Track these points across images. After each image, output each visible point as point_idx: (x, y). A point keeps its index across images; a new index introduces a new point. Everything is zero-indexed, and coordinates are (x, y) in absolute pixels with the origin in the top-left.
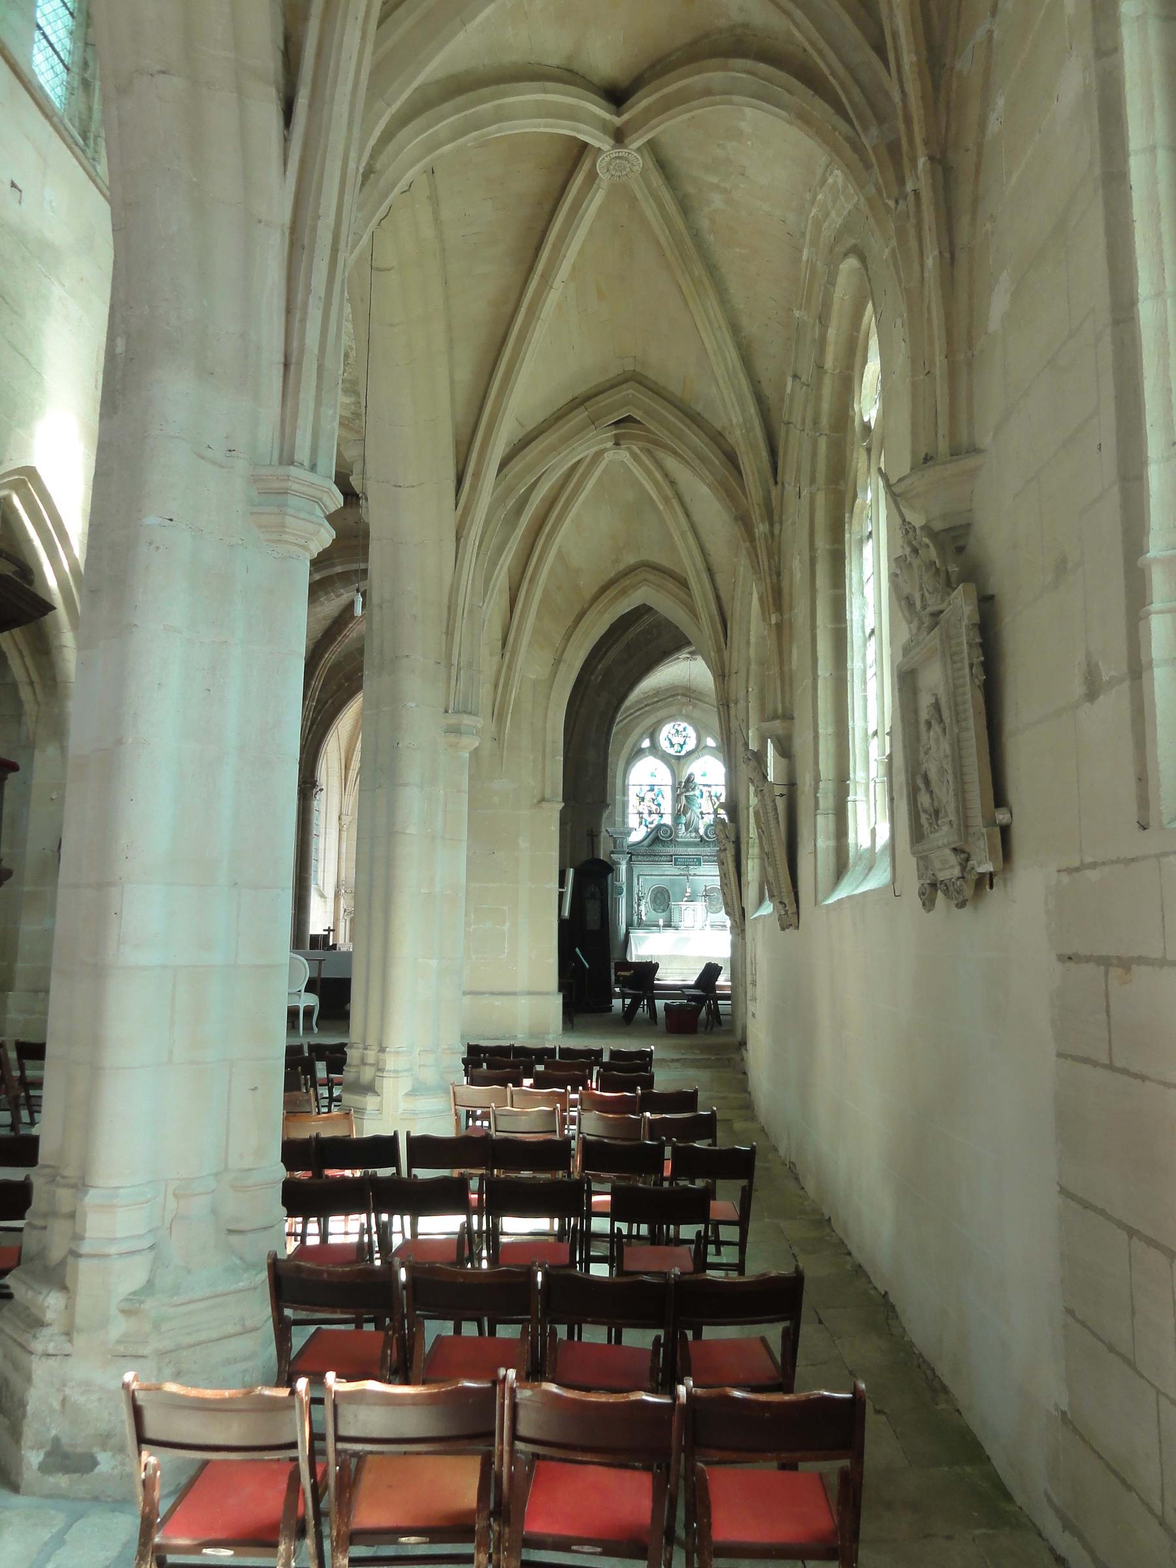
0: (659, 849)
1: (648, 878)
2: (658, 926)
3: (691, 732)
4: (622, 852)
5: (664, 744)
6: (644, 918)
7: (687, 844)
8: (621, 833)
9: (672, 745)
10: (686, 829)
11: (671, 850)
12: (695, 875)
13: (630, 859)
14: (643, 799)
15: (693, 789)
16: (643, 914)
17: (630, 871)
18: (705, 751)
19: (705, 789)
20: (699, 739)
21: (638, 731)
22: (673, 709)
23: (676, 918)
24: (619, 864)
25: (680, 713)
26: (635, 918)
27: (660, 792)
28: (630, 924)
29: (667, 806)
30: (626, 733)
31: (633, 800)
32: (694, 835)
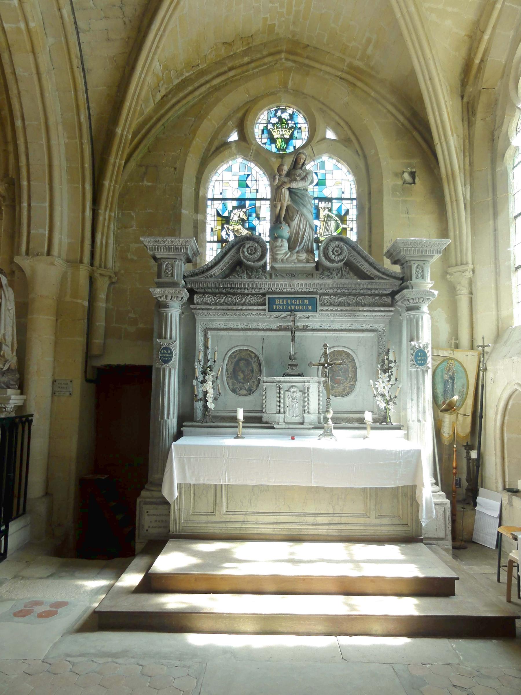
0: (242, 280)
1: (226, 331)
2: (234, 419)
3: (301, 121)
4: (174, 285)
5: (261, 139)
6: (211, 405)
7: (292, 274)
8: (169, 249)
9: (273, 140)
10: (291, 248)
11: (263, 283)
12: (305, 329)
13: (191, 300)
14: (227, 220)
15: (303, 179)
16: (210, 397)
17: (190, 323)
18: (324, 145)
19: (322, 205)
20: (313, 130)
21: (218, 112)
22: (275, 78)
23: (271, 405)
24: (166, 306)
25: (287, 91)
26: (199, 405)
27: (254, 208)
28: (186, 418)
29: (263, 229)
30: (199, 111)
31: (211, 221)
32: (304, 256)
